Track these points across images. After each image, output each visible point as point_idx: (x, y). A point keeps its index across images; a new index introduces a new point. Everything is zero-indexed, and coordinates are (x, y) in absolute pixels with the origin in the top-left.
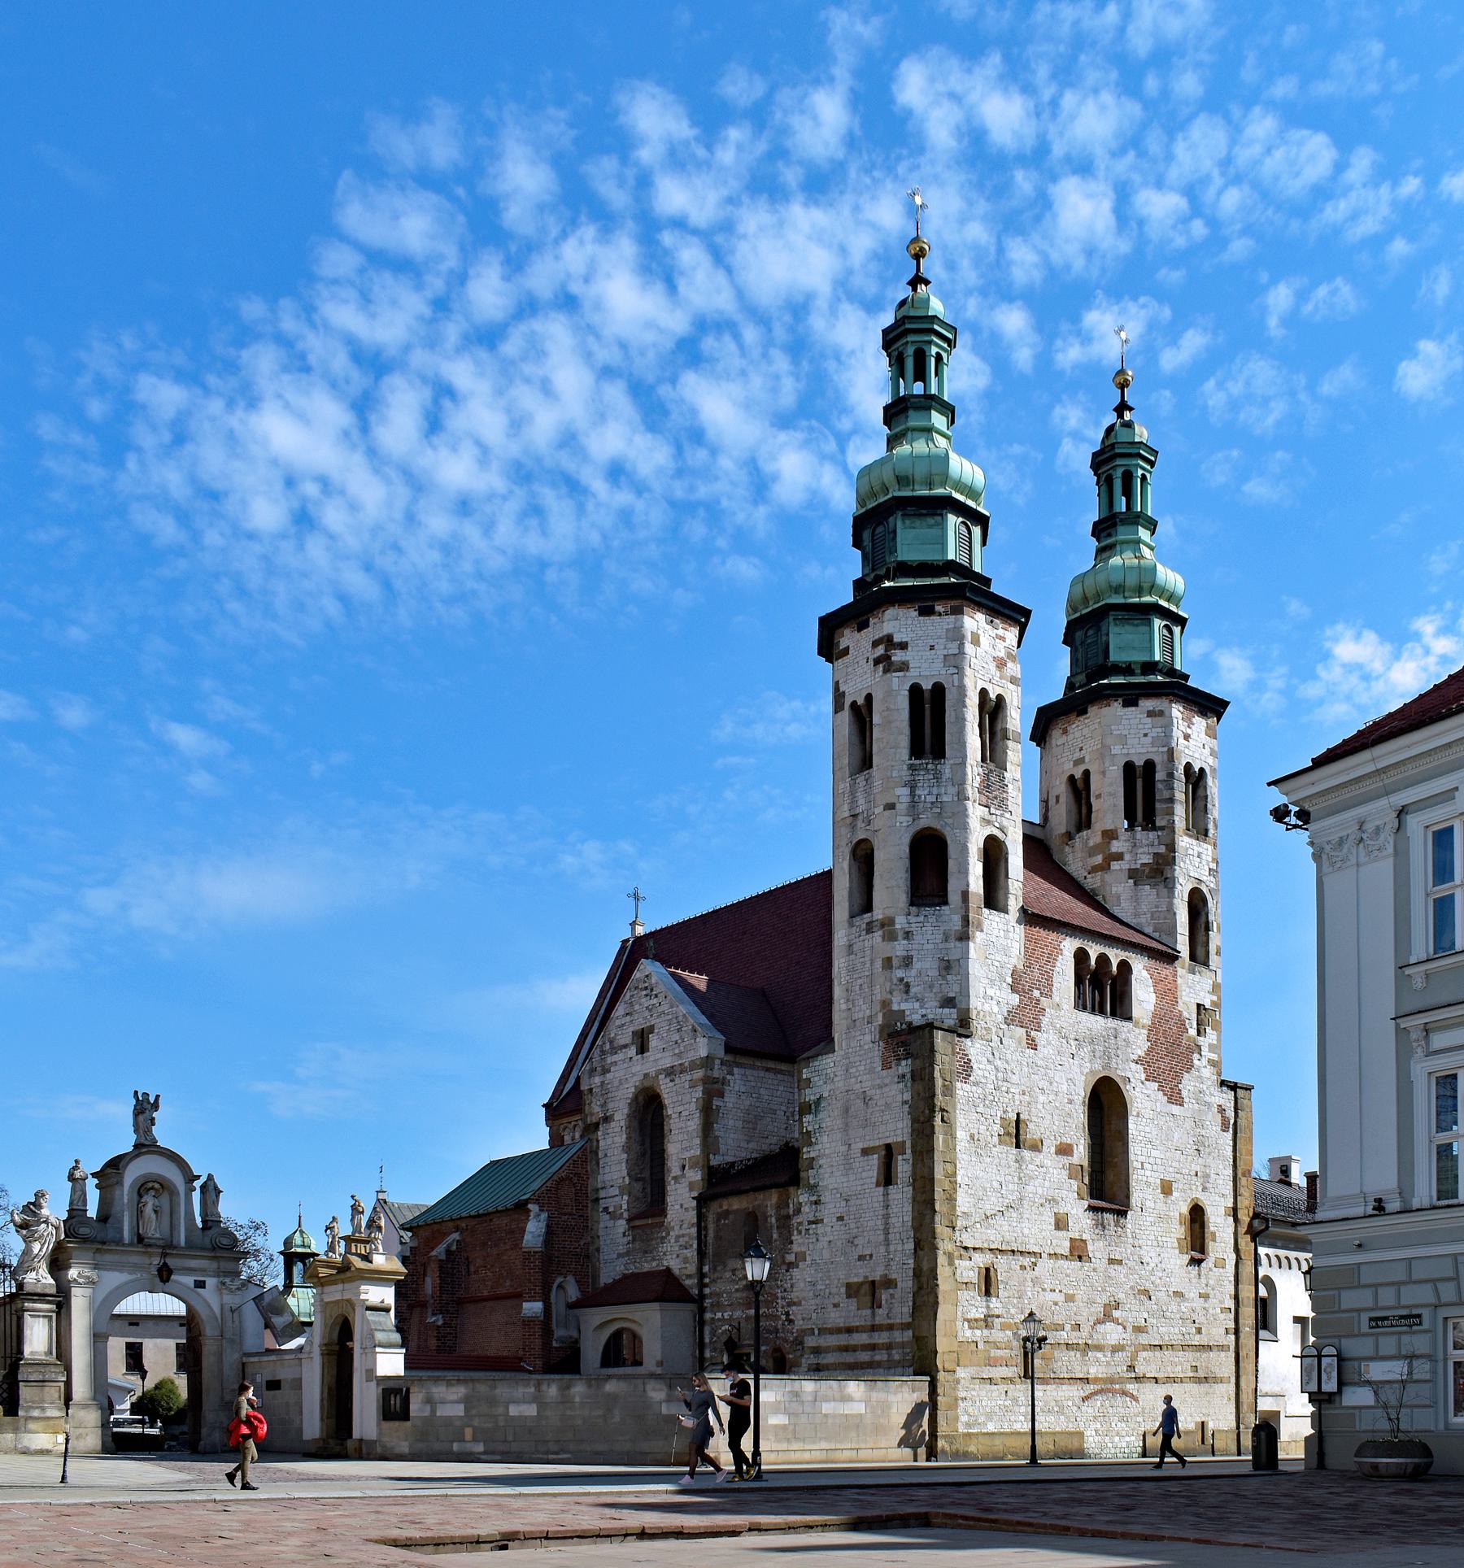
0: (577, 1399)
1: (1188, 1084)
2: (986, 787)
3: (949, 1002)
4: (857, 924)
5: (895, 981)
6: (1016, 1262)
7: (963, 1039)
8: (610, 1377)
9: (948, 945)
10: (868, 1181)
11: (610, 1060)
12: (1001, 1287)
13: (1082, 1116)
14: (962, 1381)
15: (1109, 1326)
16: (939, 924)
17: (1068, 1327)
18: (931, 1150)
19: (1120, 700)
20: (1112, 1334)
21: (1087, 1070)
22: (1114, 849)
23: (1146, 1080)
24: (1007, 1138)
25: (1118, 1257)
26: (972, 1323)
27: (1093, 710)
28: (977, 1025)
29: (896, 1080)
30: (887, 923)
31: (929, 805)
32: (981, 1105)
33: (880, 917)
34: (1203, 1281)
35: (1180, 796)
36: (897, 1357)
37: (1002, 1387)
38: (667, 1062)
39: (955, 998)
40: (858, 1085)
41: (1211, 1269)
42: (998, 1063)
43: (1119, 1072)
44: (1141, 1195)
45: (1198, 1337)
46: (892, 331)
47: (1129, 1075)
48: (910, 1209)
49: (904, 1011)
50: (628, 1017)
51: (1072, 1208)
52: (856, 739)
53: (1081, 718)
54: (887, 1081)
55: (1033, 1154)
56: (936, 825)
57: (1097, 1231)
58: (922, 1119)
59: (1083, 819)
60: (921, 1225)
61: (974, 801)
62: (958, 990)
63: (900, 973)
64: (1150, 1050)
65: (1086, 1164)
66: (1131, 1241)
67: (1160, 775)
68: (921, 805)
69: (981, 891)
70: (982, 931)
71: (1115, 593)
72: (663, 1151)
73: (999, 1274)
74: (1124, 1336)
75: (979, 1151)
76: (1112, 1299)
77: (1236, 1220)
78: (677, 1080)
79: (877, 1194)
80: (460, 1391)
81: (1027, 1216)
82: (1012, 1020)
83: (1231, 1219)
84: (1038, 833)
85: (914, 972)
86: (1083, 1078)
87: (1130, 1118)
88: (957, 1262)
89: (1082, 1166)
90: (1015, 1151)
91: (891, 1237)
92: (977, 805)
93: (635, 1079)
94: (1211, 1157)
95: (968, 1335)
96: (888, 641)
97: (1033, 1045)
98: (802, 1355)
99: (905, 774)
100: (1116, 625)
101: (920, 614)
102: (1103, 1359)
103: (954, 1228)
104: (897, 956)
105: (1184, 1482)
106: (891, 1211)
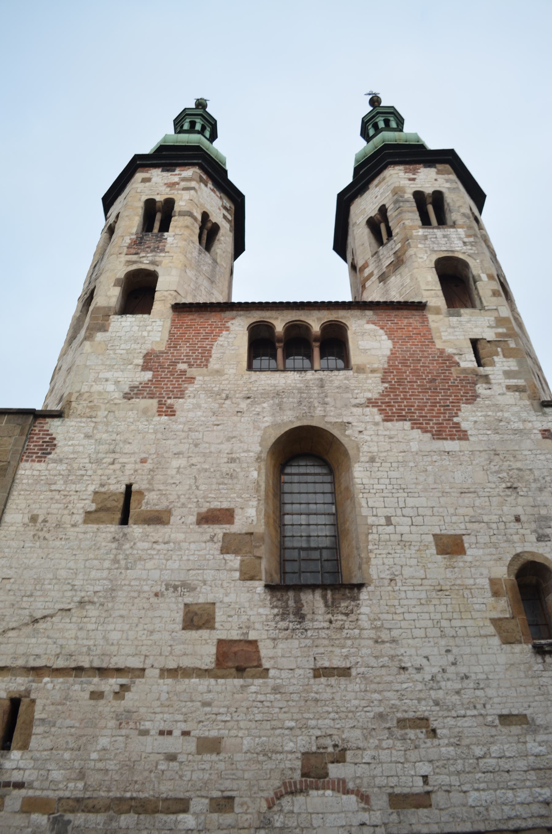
7: (48, 420)
12: (37, 730)
13: (255, 474)
23: (384, 420)
25: (337, 663)
44: (389, 561)
55: (149, 529)
57: (283, 625)
76: (328, 742)
86: (259, 433)
90: (113, 528)
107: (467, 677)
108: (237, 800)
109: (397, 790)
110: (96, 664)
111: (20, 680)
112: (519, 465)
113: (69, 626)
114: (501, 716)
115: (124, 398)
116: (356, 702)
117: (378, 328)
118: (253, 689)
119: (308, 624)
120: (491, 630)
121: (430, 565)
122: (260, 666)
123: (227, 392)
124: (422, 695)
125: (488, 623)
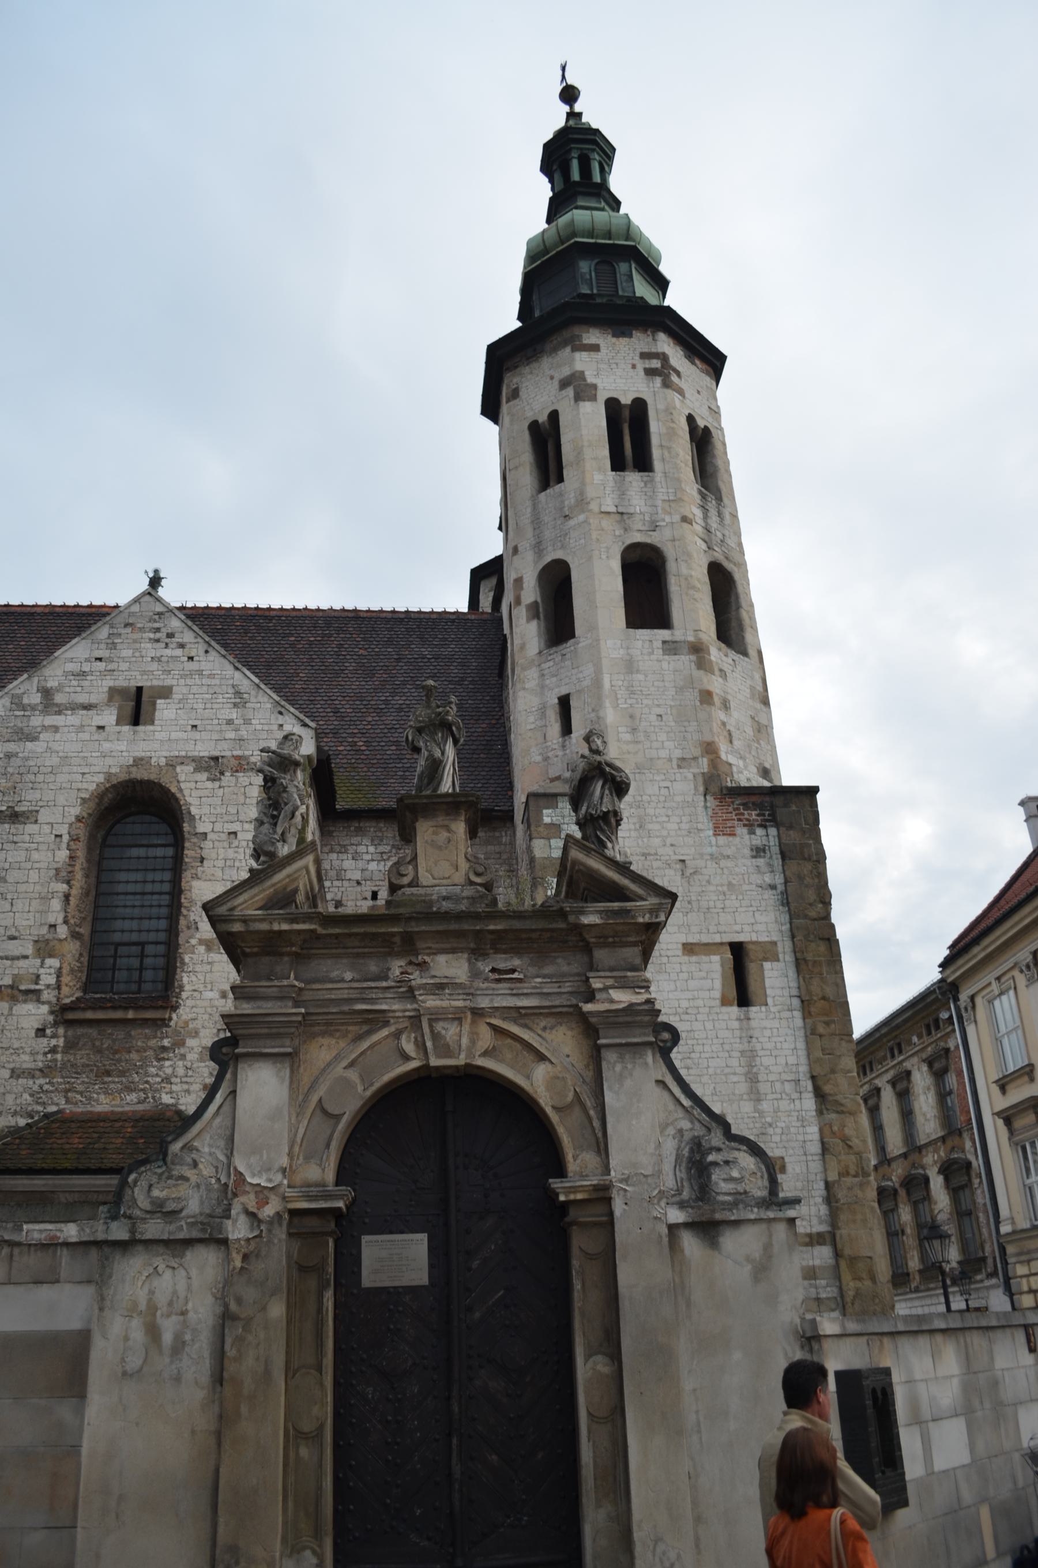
10: (706, 994)
11: (37, 721)
29: (747, 852)
30: (697, 649)
38: (204, 750)
40: (669, 851)
48: (801, 1045)
49: (730, 765)
50: (101, 665)
54: (729, 852)
58: (813, 914)
60: (833, 1071)
62: (771, 762)
72: (180, 892)
78: (227, 778)
79: (726, 1017)
91: (763, 1088)
93: (109, 761)
106: (758, 1046)
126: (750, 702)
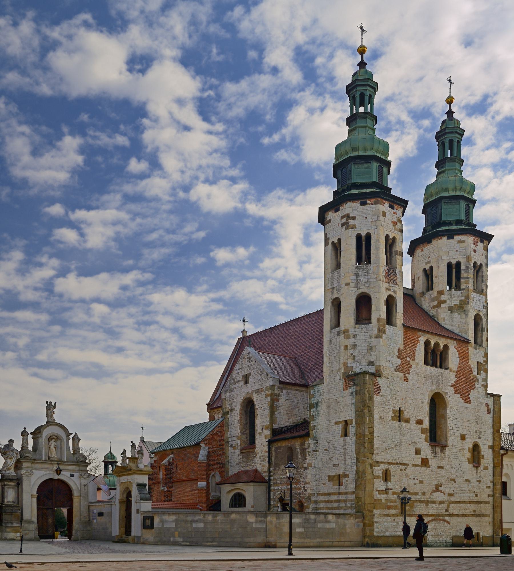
0: (220, 521)
1: (473, 395)
2: (388, 275)
3: (371, 363)
4: (334, 332)
5: (349, 355)
6: (398, 468)
7: (377, 378)
8: (233, 513)
9: (371, 340)
12: (392, 477)
14: (376, 515)
15: (438, 493)
16: (368, 332)
17: (420, 494)
18: (363, 423)
19: (446, 237)
20: (438, 496)
21: (429, 390)
22: (442, 299)
23: (455, 393)
24: (395, 418)
25: (442, 465)
26: (380, 492)
27: (434, 242)
28: (384, 373)
31: (364, 283)
32: (385, 405)
33: (343, 329)
34: (479, 475)
35: (472, 276)
36: (349, 505)
37: (393, 518)
39: (374, 361)
41: (482, 471)
42: (392, 387)
43: (443, 390)
45: (476, 497)
46: (351, 86)
47: (447, 391)
51: (423, 446)
52: (334, 257)
53: (429, 245)
55: (406, 424)
56: (366, 291)
57: (433, 455)
59: (430, 286)
60: (359, 452)
61: (383, 281)
63: (351, 352)
64: (457, 381)
65: (428, 428)
66: (447, 459)
67: (463, 267)
68: (361, 283)
69: (386, 318)
70: (386, 334)
71: (445, 191)
73: (391, 472)
74: (444, 497)
75: (384, 423)
76: (439, 482)
77: (494, 451)
80: (173, 518)
81: (404, 449)
82: (398, 370)
83: (491, 450)
84: (410, 293)
85: (357, 351)
86: (428, 393)
87: (448, 409)
88: (374, 468)
89: (427, 428)
90: (398, 423)
92: (384, 283)
94: (482, 425)
95: (378, 496)
96: (348, 216)
97: (406, 380)
98: (310, 504)
99: (354, 271)
100: (445, 205)
101: (361, 205)
102: (435, 507)
103: (373, 454)
104: (350, 345)
105: (467, 558)
107: (462, 471)
108: (426, 493)
109: (449, 493)
110: (400, 462)
111: (387, 465)
112: (479, 414)
113: (394, 452)
114: (466, 480)
115: (395, 371)
116: (444, 475)
117: (457, 351)
118: (428, 470)
119: (437, 455)
120: (467, 460)
121: (459, 442)
122: (429, 465)
123: (420, 374)
124: (454, 474)
125: (467, 459)
126: (369, 340)
